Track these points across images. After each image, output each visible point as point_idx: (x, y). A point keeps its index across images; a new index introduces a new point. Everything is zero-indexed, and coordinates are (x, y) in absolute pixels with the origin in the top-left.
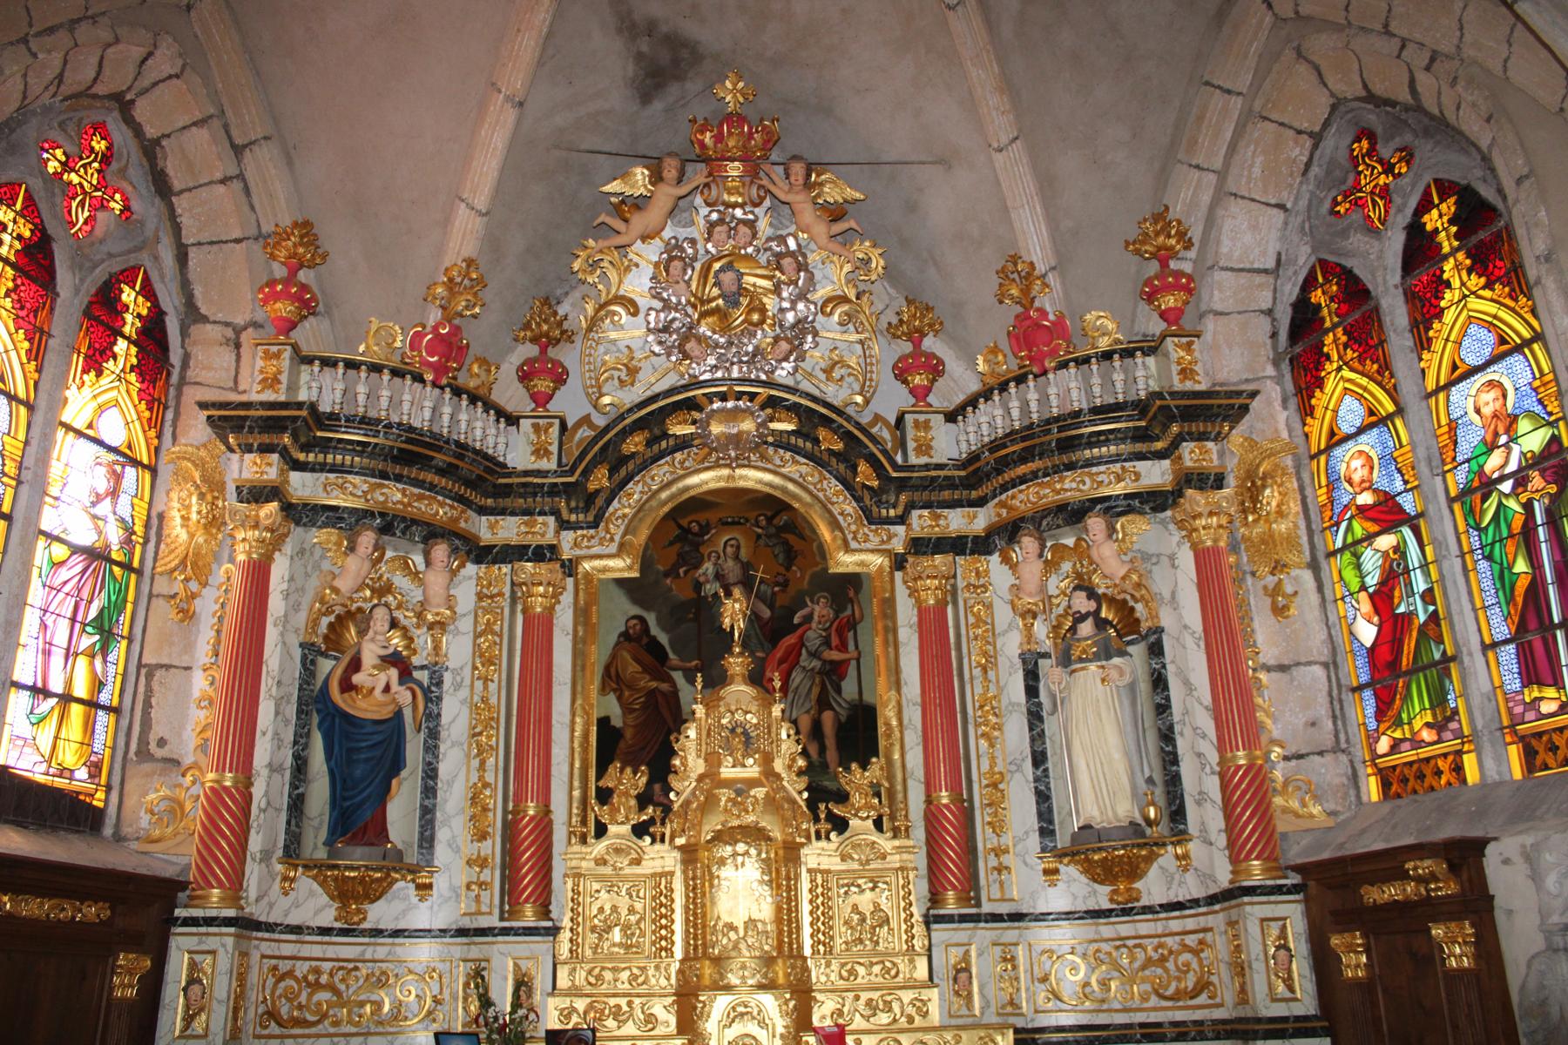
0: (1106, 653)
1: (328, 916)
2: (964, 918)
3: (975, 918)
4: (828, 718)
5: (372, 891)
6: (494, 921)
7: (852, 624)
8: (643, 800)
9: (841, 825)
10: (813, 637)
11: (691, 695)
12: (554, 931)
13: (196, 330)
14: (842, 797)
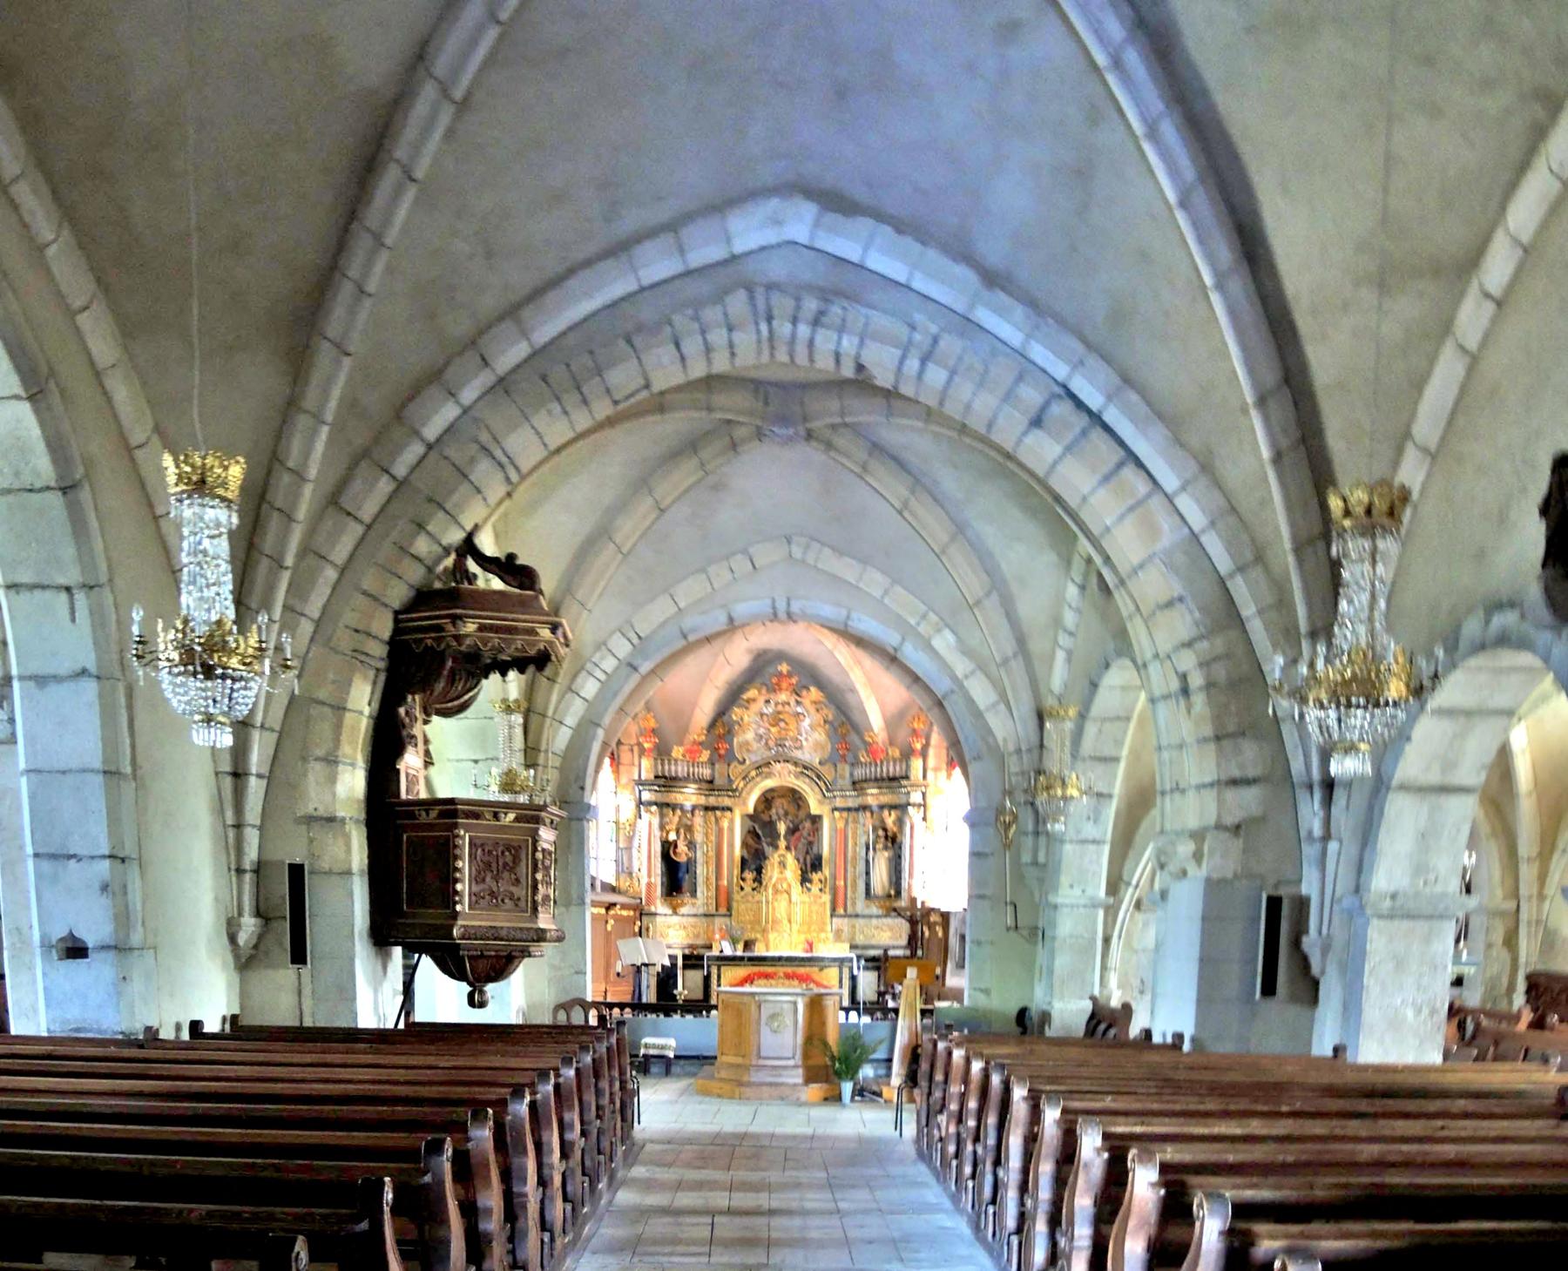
0: (886, 848)
1: (670, 912)
2: (841, 916)
3: (844, 916)
4: (808, 858)
5: (683, 904)
6: (714, 912)
7: (817, 830)
8: (754, 880)
9: (809, 890)
10: (805, 833)
11: (768, 850)
12: (730, 915)
13: (622, 747)
14: (810, 881)
